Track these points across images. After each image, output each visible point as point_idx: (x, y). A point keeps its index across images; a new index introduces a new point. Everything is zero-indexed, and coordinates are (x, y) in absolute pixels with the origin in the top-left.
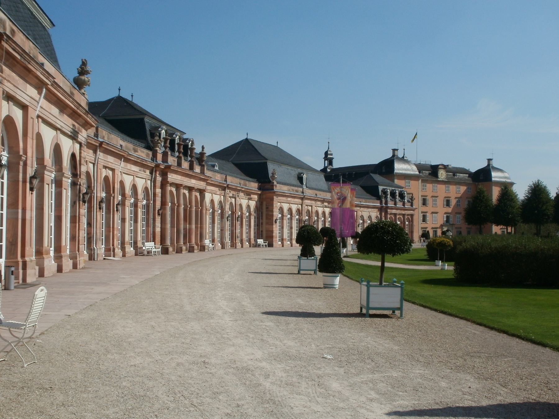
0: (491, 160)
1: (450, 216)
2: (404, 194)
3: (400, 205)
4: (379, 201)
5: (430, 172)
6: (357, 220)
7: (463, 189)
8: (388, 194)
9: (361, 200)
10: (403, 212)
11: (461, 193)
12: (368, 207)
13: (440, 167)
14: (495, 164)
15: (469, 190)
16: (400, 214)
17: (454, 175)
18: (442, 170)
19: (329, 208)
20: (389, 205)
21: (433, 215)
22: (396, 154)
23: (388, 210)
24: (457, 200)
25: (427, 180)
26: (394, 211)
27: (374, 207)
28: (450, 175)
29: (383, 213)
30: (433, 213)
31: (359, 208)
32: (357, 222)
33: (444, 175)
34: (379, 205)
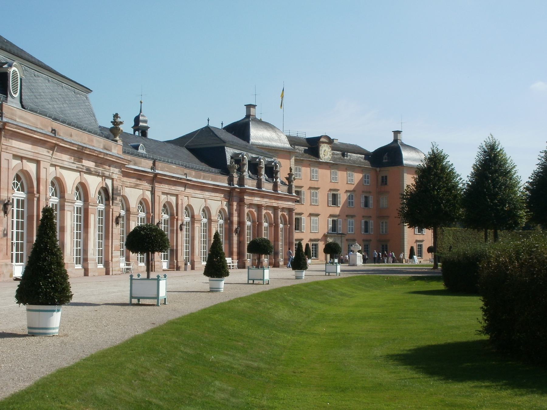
0: (399, 132)
1: (337, 220)
2: (276, 168)
3: (267, 187)
4: (226, 178)
5: (307, 148)
6: (177, 215)
7: (357, 177)
8: (244, 165)
9: (187, 171)
10: (275, 203)
11: (354, 184)
12: (202, 188)
13: (322, 140)
14: (404, 138)
15: (367, 180)
16: (268, 207)
17: (343, 155)
18: (326, 145)
19: (98, 175)
20: (246, 186)
21: (312, 218)
22: (251, 114)
23: (245, 197)
24: (349, 194)
25: (303, 160)
26: (257, 200)
27: (216, 189)
28: (337, 154)
29: (235, 204)
30: (311, 215)
31: (183, 189)
32: (177, 220)
33: (329, 155)
34: (227, 185)
